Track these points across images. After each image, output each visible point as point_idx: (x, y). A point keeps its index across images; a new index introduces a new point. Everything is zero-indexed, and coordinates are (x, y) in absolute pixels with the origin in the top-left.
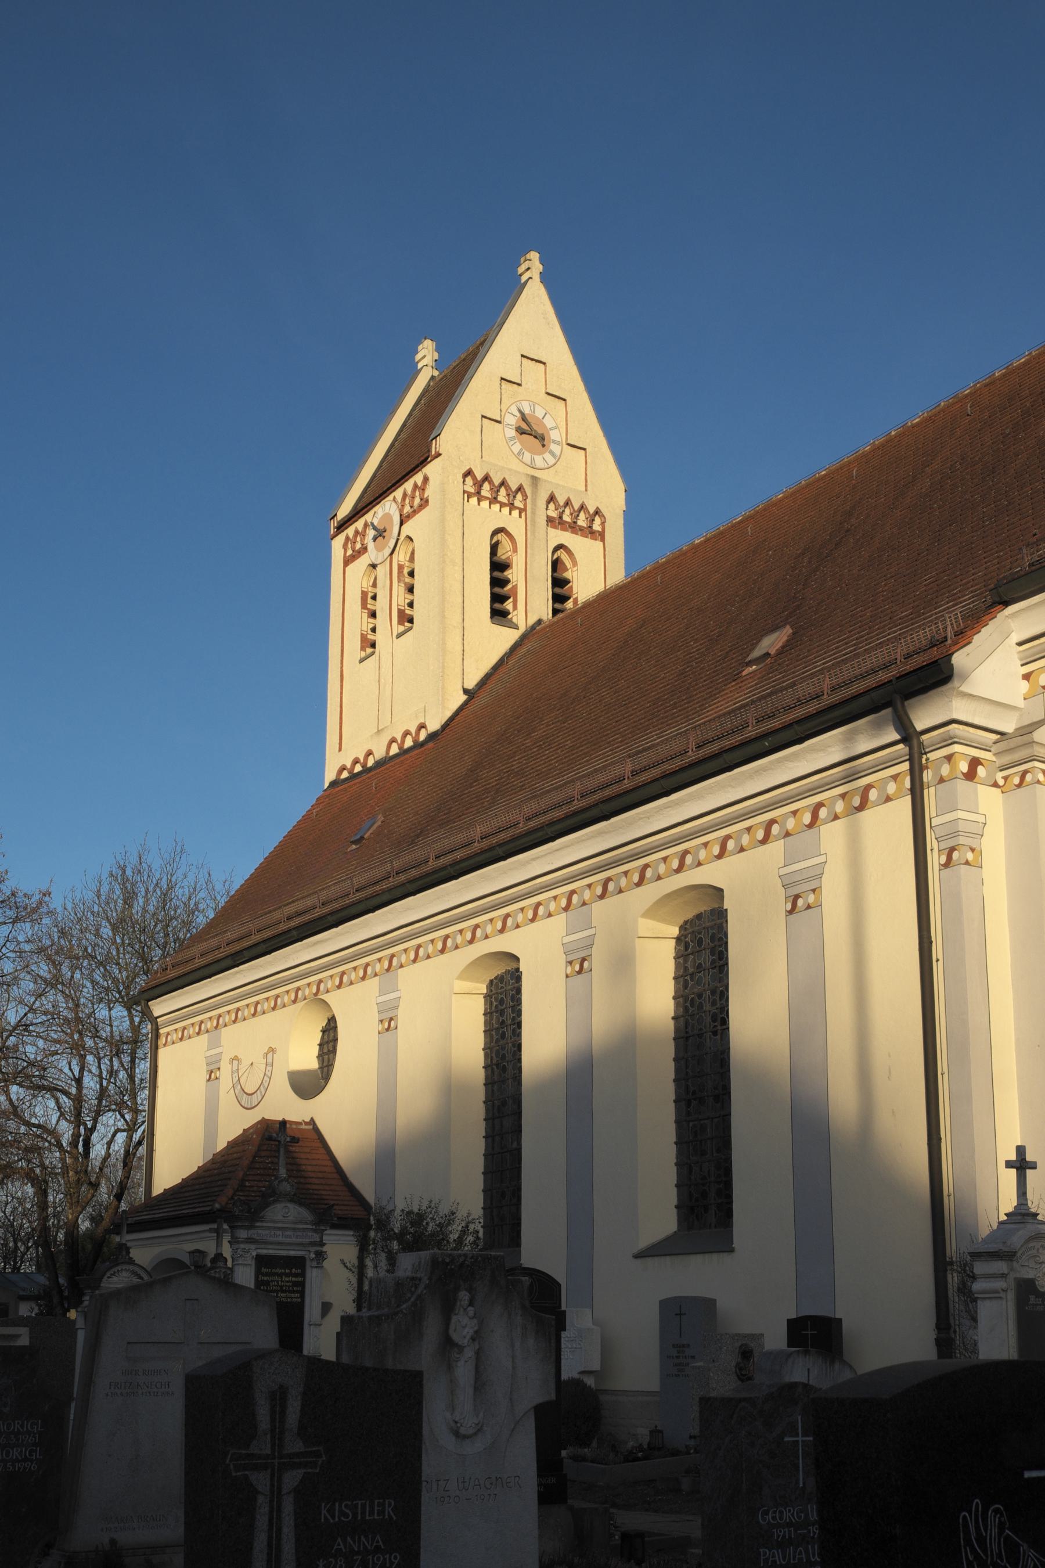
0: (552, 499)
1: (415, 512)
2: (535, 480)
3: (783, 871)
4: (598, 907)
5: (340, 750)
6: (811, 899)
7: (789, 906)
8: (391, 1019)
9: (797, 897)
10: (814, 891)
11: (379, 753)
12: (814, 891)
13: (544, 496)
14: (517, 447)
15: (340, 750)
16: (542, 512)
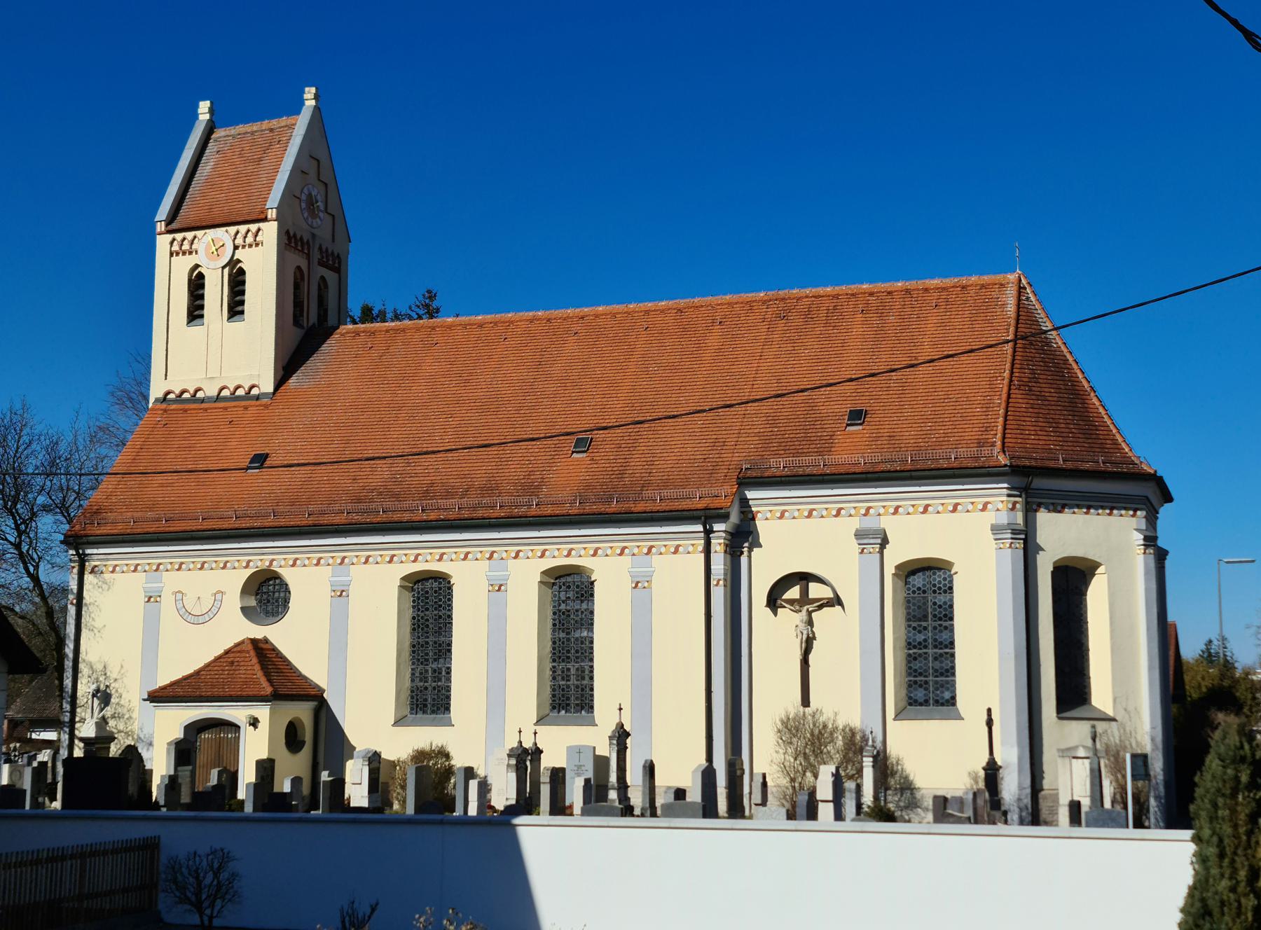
0: (320, 248)
1: (244, 247)
2: (314, 235)
3: (632, 570)
4: (511, 562)
5: (166, 379)
6: (646, 584)
7: (634, 585)
8: (343, 591)
9: (638, 582)
10: (648, 581)
11: (211, 391)
12: (648, 581)
13: (317, 246)
14: (306, 215)
15: (166, 379)
16: (316, 256)
